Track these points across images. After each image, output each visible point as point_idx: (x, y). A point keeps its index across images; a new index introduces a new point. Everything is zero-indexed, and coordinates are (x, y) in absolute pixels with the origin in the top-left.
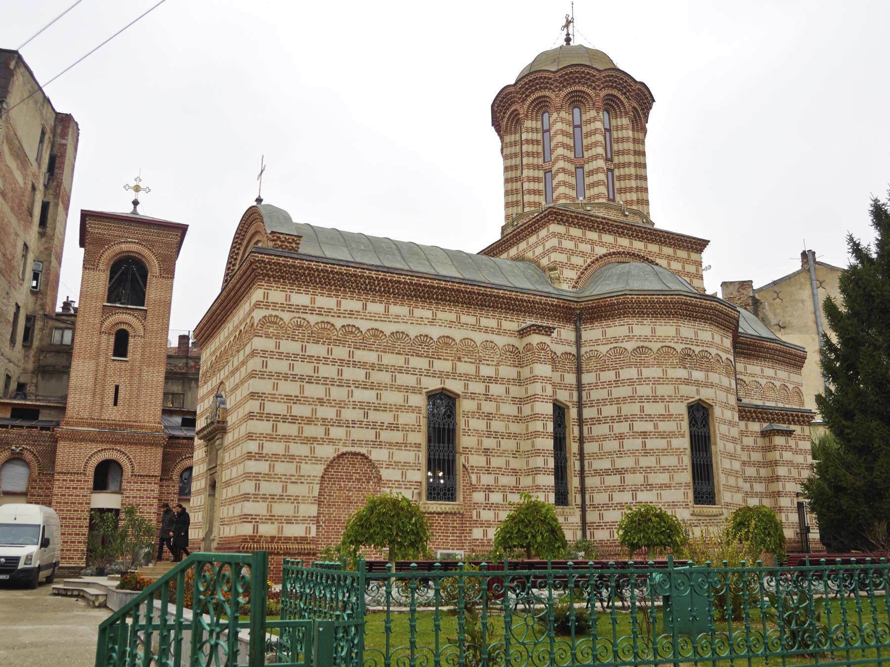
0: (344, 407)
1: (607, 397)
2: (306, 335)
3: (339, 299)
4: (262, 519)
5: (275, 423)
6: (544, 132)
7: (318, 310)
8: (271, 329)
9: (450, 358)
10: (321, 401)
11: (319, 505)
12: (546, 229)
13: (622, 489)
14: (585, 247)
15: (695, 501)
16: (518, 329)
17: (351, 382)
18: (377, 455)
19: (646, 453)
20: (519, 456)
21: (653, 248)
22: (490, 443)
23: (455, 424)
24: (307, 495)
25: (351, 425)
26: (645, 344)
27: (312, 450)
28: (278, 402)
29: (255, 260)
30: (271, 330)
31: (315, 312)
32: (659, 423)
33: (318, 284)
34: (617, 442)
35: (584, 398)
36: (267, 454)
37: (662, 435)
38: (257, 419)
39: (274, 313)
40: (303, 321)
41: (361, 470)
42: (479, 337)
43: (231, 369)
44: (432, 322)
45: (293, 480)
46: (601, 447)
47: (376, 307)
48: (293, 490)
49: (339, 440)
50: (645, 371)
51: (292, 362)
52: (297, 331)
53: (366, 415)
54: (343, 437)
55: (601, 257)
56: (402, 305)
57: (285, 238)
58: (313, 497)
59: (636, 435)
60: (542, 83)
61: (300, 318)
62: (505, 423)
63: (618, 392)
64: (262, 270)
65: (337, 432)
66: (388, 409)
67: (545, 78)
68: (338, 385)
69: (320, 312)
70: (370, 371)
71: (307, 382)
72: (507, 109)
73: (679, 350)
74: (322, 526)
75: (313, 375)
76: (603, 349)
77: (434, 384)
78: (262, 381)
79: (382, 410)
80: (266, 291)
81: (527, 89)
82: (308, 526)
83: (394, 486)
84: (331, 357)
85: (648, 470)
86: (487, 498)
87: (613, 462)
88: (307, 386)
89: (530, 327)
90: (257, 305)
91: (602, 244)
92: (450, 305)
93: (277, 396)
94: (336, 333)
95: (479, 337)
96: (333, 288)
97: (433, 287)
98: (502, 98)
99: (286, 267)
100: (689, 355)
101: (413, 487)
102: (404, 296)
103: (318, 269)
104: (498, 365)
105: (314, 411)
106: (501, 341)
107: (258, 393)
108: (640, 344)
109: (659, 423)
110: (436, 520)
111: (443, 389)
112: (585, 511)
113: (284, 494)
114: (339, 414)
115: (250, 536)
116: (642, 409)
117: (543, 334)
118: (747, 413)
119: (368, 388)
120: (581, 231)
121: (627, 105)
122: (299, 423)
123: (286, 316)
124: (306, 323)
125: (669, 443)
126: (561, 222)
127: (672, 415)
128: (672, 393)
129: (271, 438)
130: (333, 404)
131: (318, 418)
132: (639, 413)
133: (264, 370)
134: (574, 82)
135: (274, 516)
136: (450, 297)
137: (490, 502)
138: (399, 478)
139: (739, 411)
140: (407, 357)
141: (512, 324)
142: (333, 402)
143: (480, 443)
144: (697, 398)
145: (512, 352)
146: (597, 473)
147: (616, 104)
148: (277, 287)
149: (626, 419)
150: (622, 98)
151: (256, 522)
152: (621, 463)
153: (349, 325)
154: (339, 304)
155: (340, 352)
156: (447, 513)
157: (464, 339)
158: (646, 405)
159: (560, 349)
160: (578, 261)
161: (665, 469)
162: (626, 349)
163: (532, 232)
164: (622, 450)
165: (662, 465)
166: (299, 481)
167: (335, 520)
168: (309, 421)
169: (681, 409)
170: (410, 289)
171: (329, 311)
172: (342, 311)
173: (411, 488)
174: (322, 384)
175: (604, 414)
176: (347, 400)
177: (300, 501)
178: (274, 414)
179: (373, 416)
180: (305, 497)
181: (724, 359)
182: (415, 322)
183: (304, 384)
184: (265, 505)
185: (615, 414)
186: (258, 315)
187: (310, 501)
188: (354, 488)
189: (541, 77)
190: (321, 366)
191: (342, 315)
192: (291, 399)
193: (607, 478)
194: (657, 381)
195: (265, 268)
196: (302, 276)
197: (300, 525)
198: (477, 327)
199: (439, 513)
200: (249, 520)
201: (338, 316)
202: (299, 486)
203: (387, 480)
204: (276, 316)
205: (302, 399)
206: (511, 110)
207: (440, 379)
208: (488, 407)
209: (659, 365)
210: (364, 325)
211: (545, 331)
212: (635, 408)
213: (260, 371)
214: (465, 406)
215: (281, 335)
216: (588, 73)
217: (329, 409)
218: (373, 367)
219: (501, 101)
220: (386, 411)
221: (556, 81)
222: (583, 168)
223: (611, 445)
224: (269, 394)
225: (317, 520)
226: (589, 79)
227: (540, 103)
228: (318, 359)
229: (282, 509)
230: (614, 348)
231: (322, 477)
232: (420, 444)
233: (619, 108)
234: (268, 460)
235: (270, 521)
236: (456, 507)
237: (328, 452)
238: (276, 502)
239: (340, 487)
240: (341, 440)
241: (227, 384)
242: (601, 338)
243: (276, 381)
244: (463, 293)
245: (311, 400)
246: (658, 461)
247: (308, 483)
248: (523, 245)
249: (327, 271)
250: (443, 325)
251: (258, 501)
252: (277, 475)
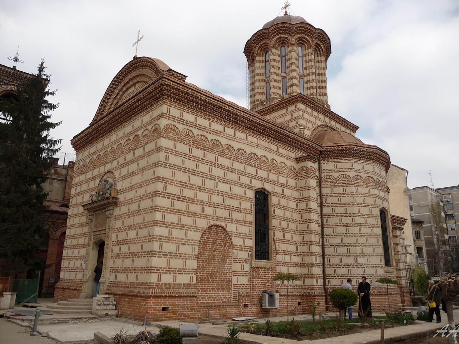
0: (212, 194)
1: (338, 202)
2: (192, 142)
3: (210, 122)
4: (163, 270)
5: (173, 200)
6: (282, 57)
7: (198, 126)
8: (171, 134)
9: (266, 170)
10: (200, 188)
11: (198, 260)
12: (294, 106)
13: (348, 256)
14: (312, 119)
15: (385, 264)
16: (295, 157)
17: (217, 177)
18: (231, 228)
19: (362, 235)
20: (297, 234)
21: (338, 126)
22: (284, 224)
23: (268, 211)
24: (191, 253)
25: (216, 206)
26: (359, 174)
27: (195, 222)
28: (175, 185)
29: (165, 83)
30: (171, 135)
31: (197, 127)
32: (368, 219)
33: (199, 109)
34: (344, 228)
35: (324, 202)
36: (167, 223)
37: (369, 226)
38: (161, 197)
39: (173, 123)
40: (190, 132)
41: (221, 238)
42: (279, 159)
43: (122, 161)
44: (258, 145)
45: (183, 242)
46: (334, 231)
47: (230, 131)
48: (184, 249)
49: (210, 216)
50: (359, 189)
51: (183, 159)
52: (186, 138)
53: (224, 200)
54: (212, 214)
55: (319, 126)
56: (242, 132)
57: (177, 76)
58: (195, 255)
59: (355, 225)
60: (284, 30)
61: (188, 129)
62: (290, 213)
63: (345, 200)
64: (168, 92)
65: (209, 211)
66: (236, 198)
67: (287, 27)
68: (209, 179)
69: (200, 128)
70: (227, 171)
71: (192, 174)
72: (260, 42)
73: (375, 179)
74: (199, 276)
75: (195, 169)
76: (335, 175)
77: (258, 184)
78: (166, 169)
79: (233, 198)
80: (169, 107)
81: (275, 32)
82: (192, 275)
83: (239, 249)
84: (206, 159)
85: (363, 245)
86: (283, 259)
87: (342, 240)
88: (192, 177)
89: (306, 157)
90: (162, 116)
91: (320, 120)
92: (266, 137)
93: (174, 181)
94: (208, 144)
95: (279, 159)
96: (207, 113)
97: (259, 124)
98: (258, 36)
99: (182, 93)
101: (249, 250)
102: (244, 127)
103: (201, 99)
104: (287, 177)
105: (196, 195)
106: (289, 163)
107: (163, 178)
108: (357, 174)
109: (368, 219)
110: (260, 272)
111: (263, 188)
112: (325, 268)
113: (178, 252)
114: (210, 198)
115: (155, 283)
116: (359, 210)
117: (312, 162)
119: (225, 183)
120: (311, 110)
121: (324, 50)
122: (187, 202)
123: (181, 127)
124: (192, 134)
125: (372, 230)
126: (304, 103)
127: (373, 215)
128: (373, 203)
129: (170, 211)
130: (206, 191)
131: (198, 200)
132: (357, 213)
133: (167, 161)
134: (301, 33)
135: (171, 268)
136: (266, 132)
137: (285, 261)
138: (241, 244)
140: (245, 165)
141: (293, 155)
142: (207, 190)
143: (280, 224)
145: (293, 171)
146: (332, 245)
147: (319, 49)
148: (175, 106)
149: (350, 215)
150: (322, 46)
151: (159, 273)
152: (347, 241)
153: (216, 140)
154: (210, 125)
155: (211, 157)
156: (265, 268)
157: (272, 159)
158: (360, 208)
160: (310, 126)
161: (371, 245)
162: (350, 176)
163: (283, 107)
164: (347, 233)
165: (369, 243)
166: (187, 243)
167: (207, 272)
168: (193, 201)
169: (376, 212)
170: (248, 123)
171: (205, 128)
172: (212, 130)
173: (247, 251)
174: (201, 176)
175: (336, 212)
176: (214, 189)
177: (187, 258)
178: (172, 194)
179: (230, 202)
180: (190, 255)
182: (249, 144)
183: (190, 175)
184: (165, 260)
185: (343, 212)
186: (163, 122)
187: (192, 258)
188: (217, 249)
189: (284, 26)
190: (201, 165)
191: (212, 133)
192: (182, 185)
193: (338, 248)
194: (365, 195)
195: (170, 91)
196: (191, 101)
197: (187, 275)
199: (262, 268)
200: (155, 271)
201: (210, 133)
202: (187, 246)
203: (235, 245)
204: (174, 125)
205: (189, 185)
206: (262, 43)
207: (261, 182)
208: (284, 202)
209: (366, 186)
210: (224, 142)
211: (314, 160)
212: (355, 209)
213: (164, 162)
214: (274, 200)
215: (177, 139)
216: (310, 29)
217: (204, 193)
218: (228, 169)
219: (256, 37)
220: (235, 199)
221: (293, 29)
222: (303, 79)
223: (341, 230)
224: (169, 179)
225: (196, 271)
226: (309, 32)
227: (264, 46)
228: (198, 159)
229: (176, 263)
230: (342, 174)
231: (200, 241)
232: (252, 222)
233: (320, 51)
234: (168, 227)
235: (168, 272)
236: (270, 264)
237: (203, 223)
238: (172, 258)
239: (210, 249)
240: (210, 216)
241: (117, 174)
242: (334, 168)
243: (174, 171)
244: (273, 131)
245: (194, 187)
246: (367, 241)
247: (192, 245)
248: (274, 115)
249: (206, 101)
250: (263, 149)
251: (161, 257)
252: (173, 238)
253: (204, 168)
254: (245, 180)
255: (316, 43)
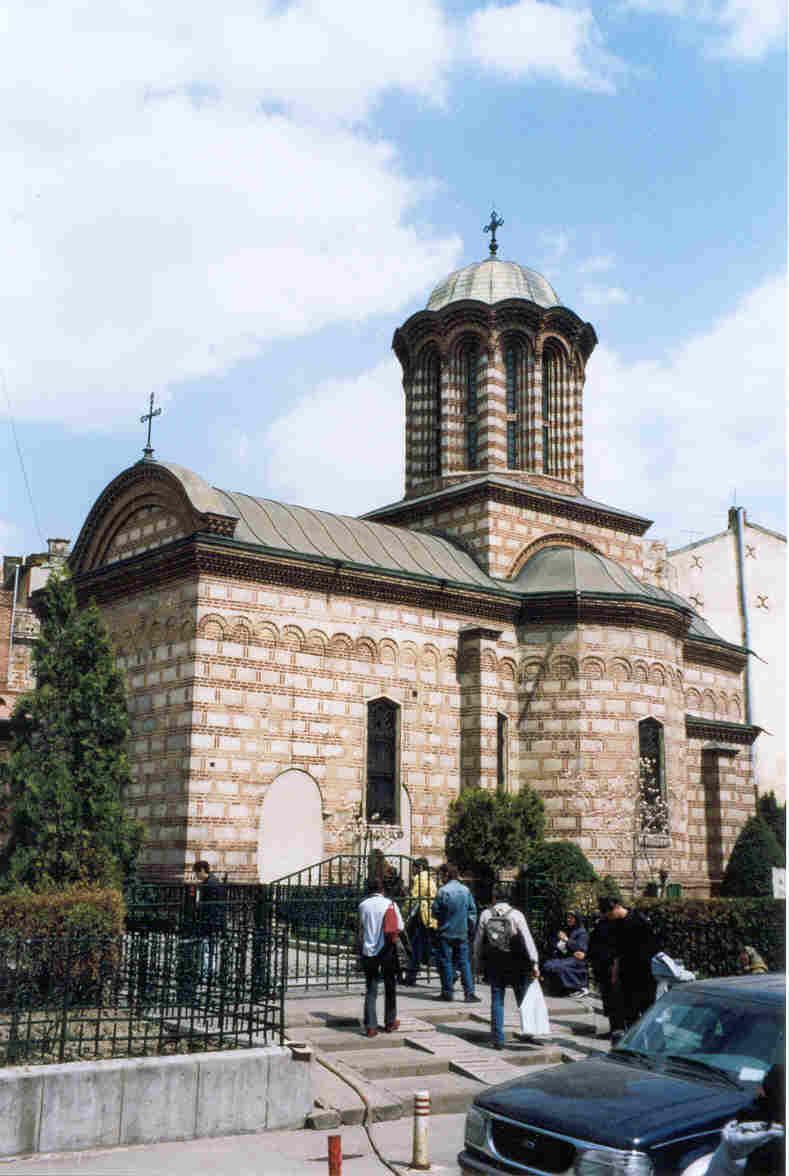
14: (522, 529)
39: (216, 611)
43: (132, 662)
95: (421, 639)
100: (641, 667)
111: (383, 698)
118: (695, 729)
126: (498, 500)
139: (687, 726)
144: (648, 716)
155: (283, 657)
159: (501, 653)
169: (631, 728)
181: (675, 670)
192: (230, 708)
198: (418, 628)
214: (406, 716)
218: (314, 672)
248: (443, 518)
253: (270, 677)
254: (345, 687)
255: (548, 338)
